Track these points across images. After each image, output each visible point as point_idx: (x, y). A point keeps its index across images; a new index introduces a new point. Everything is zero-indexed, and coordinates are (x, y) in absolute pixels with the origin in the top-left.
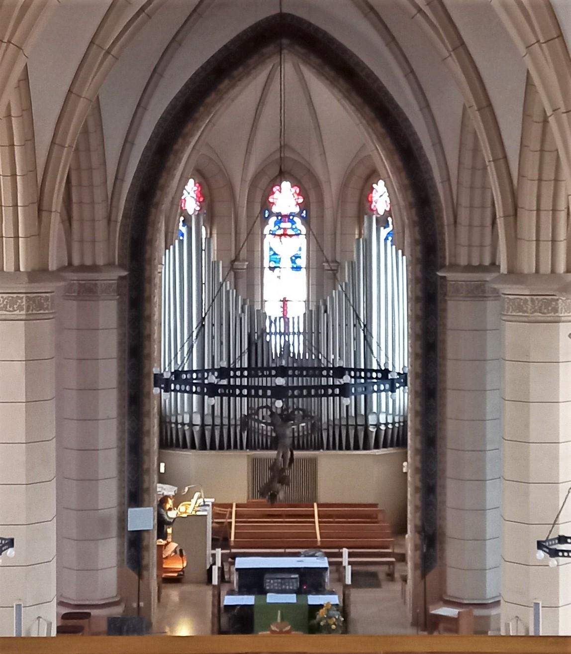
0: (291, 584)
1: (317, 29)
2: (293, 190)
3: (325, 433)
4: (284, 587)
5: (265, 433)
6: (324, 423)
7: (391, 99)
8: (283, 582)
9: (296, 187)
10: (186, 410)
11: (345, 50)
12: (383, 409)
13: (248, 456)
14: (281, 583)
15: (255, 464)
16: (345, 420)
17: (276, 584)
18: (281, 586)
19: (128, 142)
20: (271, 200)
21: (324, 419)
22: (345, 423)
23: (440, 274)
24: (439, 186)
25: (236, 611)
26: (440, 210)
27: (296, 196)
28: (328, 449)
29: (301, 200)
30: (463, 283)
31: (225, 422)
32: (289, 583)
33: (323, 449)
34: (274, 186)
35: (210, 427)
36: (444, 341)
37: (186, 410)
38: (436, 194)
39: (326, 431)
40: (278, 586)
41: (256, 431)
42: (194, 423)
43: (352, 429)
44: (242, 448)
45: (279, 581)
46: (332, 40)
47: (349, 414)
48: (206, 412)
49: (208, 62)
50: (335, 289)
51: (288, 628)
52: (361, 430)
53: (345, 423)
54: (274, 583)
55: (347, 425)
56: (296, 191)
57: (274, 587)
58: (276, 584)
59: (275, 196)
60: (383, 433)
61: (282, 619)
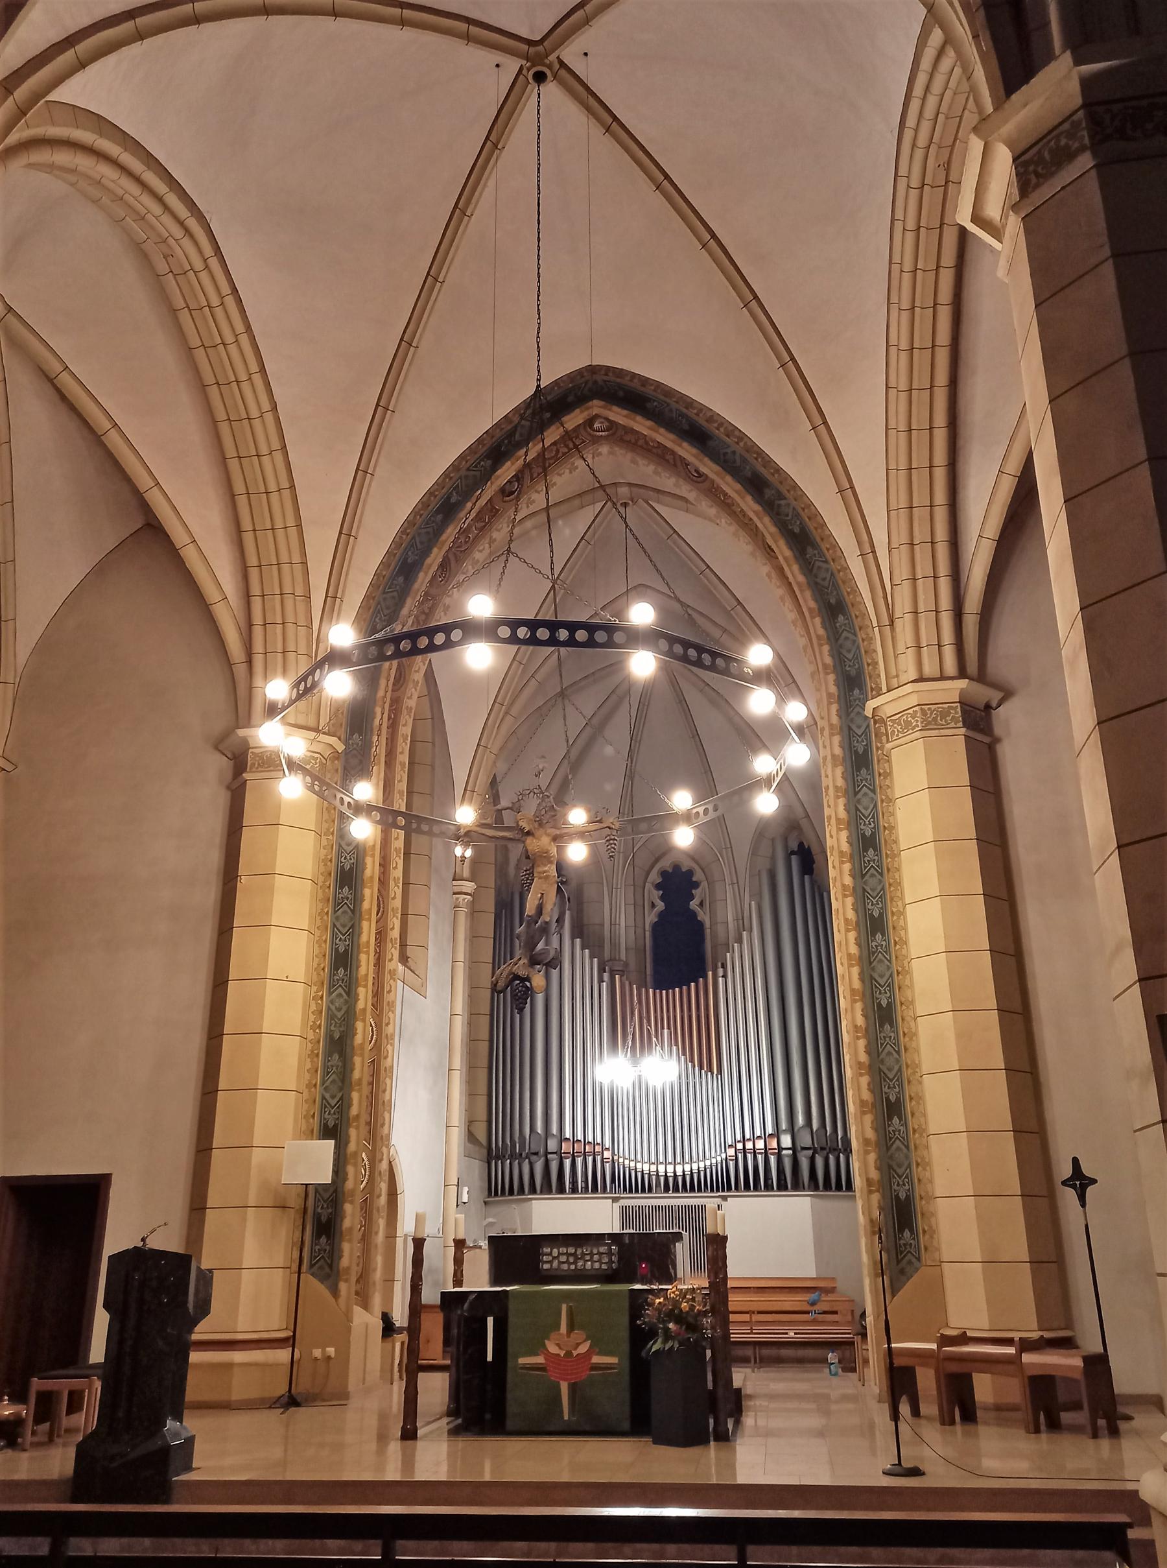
0: (596, 1257)
1: (645, 381)
4: (580, 1263)
7: (768, 462)
8: (579, 1251)
11: (690, 403)
14: (574, 1254)
15: (623, 1209)
17: (563, 1259)
18: (575, 1263)
19: (346, 534)
23: (871, 705)
24: (856, 567)
25: (466, 1306)
26: (865, 615)
30: (916, 708)
32: (591, 1254)
33: (729, 1189)
36: (892, 828)
38: (855, 590)
40: (567, 1262)
45: (571, 1250)
46: (669, 392)
49: (480, 441)
51: (584, 1348)
52: (787, 1155)
54: (559, 1254)
57: (561, 1263)
58: (563, 1259)
61: (571, 1327)
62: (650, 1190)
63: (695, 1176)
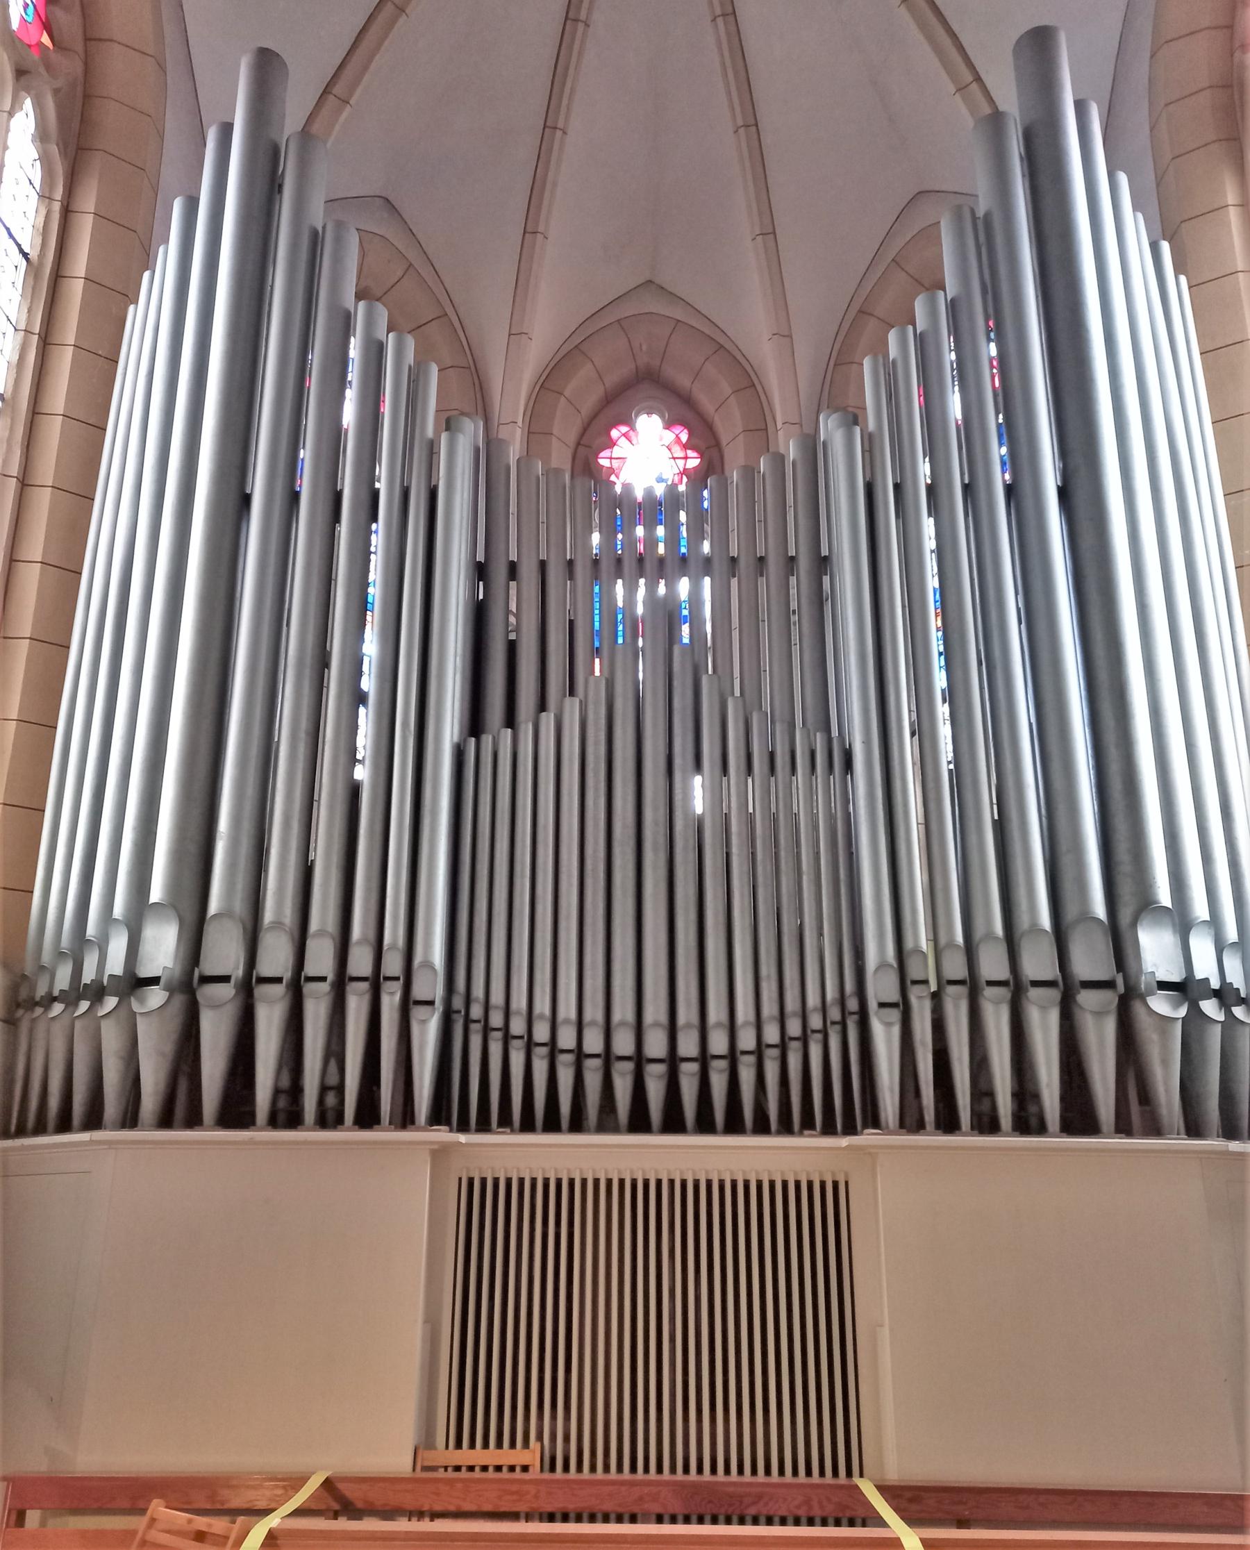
2: (669, 436)
3: (888, 1025)
5: (541, 1033)
6: (882, 965)
9: (678, 429)
10: (118, 910)
12: (1200, 910)
13: (440, 1154)
16: (1001, 952)
20: (604, 462)
21: (878, 949)
22: (1003, 973)
27: (679, 452)
28: (911, 1121)
29: (693, 463)
31: (321, 960)
34: (615, 425)
35: (226, 992)
37: (118, 910)
39: (895, 1015)
41: (496, 1020)
42: (145, 972)
43: (1044, 1008)
44: (406, 1119)
47: (1023, 921)
48: (214, 906)
50: (870, 436)
53: (1003, 973)
55: (1016, 988)
56: (678, 438)
59: (616, 452)
60: (1215, 1037)
62: (577, 1125)
63: (747, 1076)
